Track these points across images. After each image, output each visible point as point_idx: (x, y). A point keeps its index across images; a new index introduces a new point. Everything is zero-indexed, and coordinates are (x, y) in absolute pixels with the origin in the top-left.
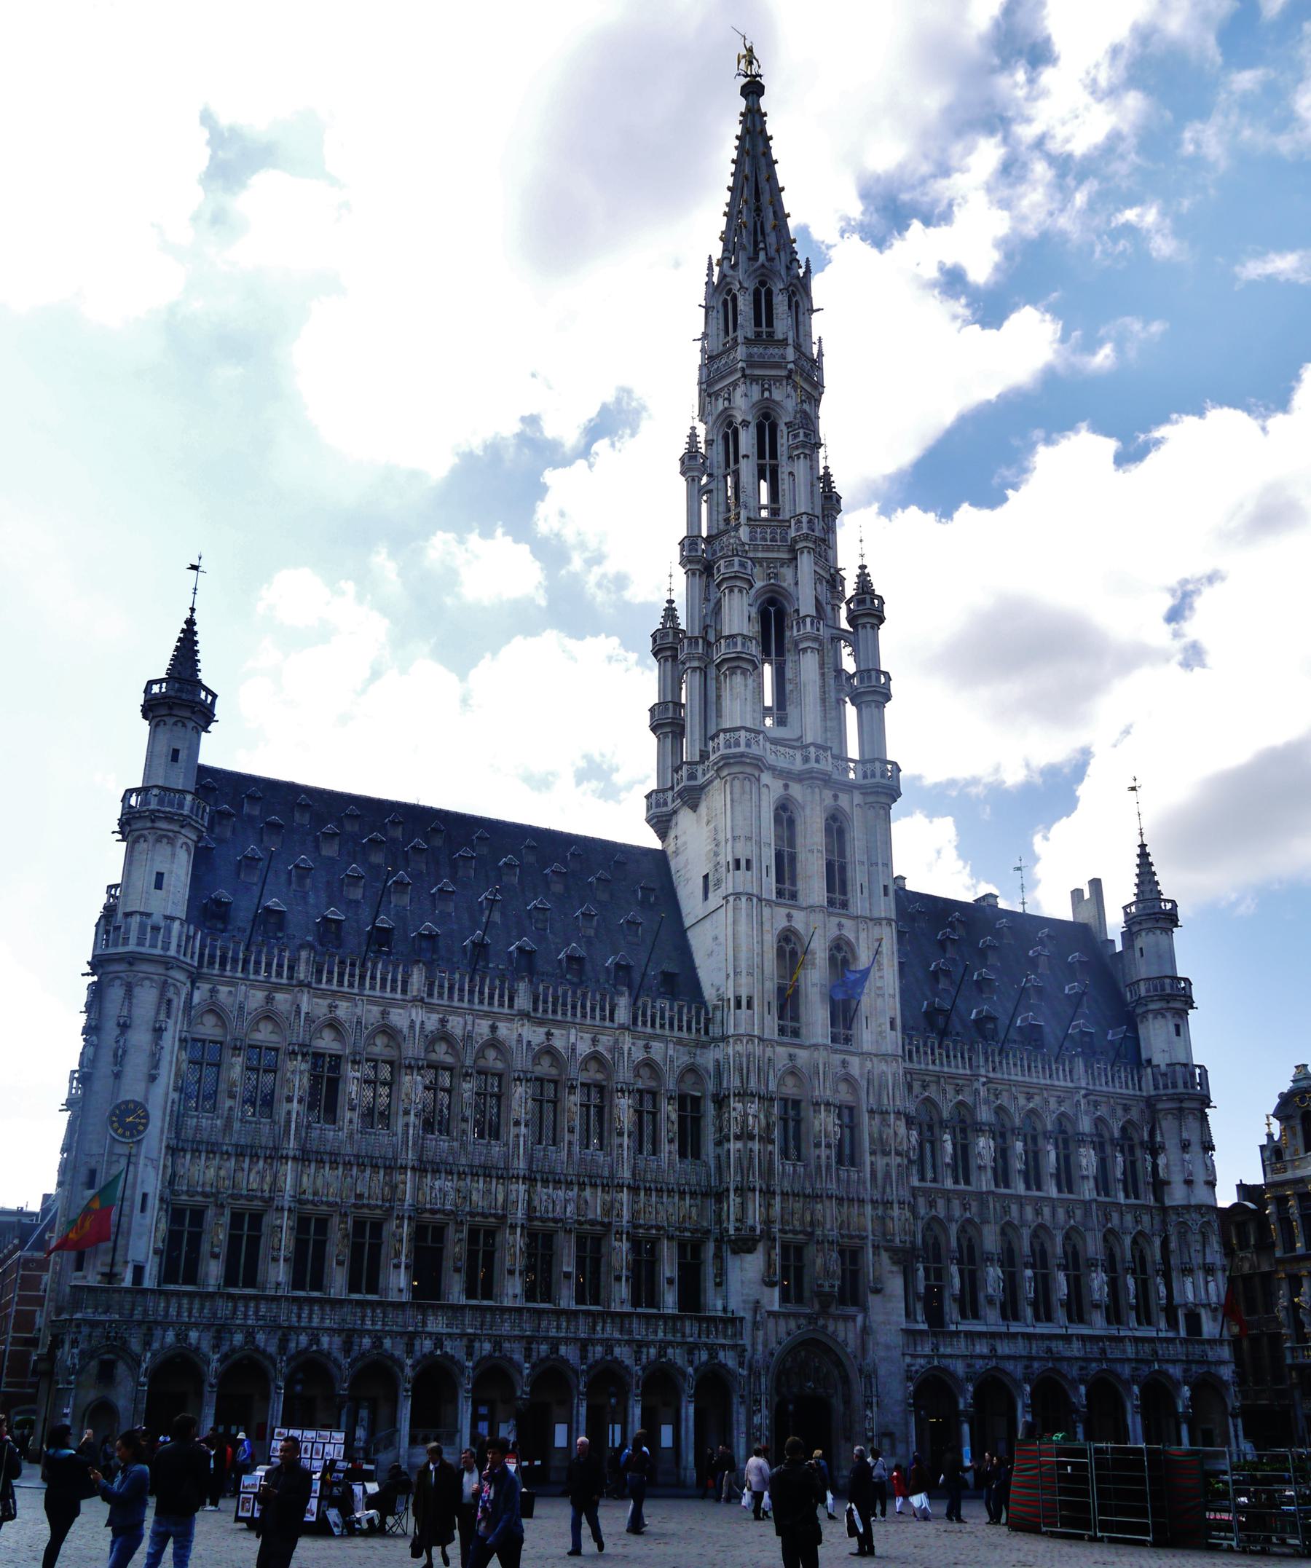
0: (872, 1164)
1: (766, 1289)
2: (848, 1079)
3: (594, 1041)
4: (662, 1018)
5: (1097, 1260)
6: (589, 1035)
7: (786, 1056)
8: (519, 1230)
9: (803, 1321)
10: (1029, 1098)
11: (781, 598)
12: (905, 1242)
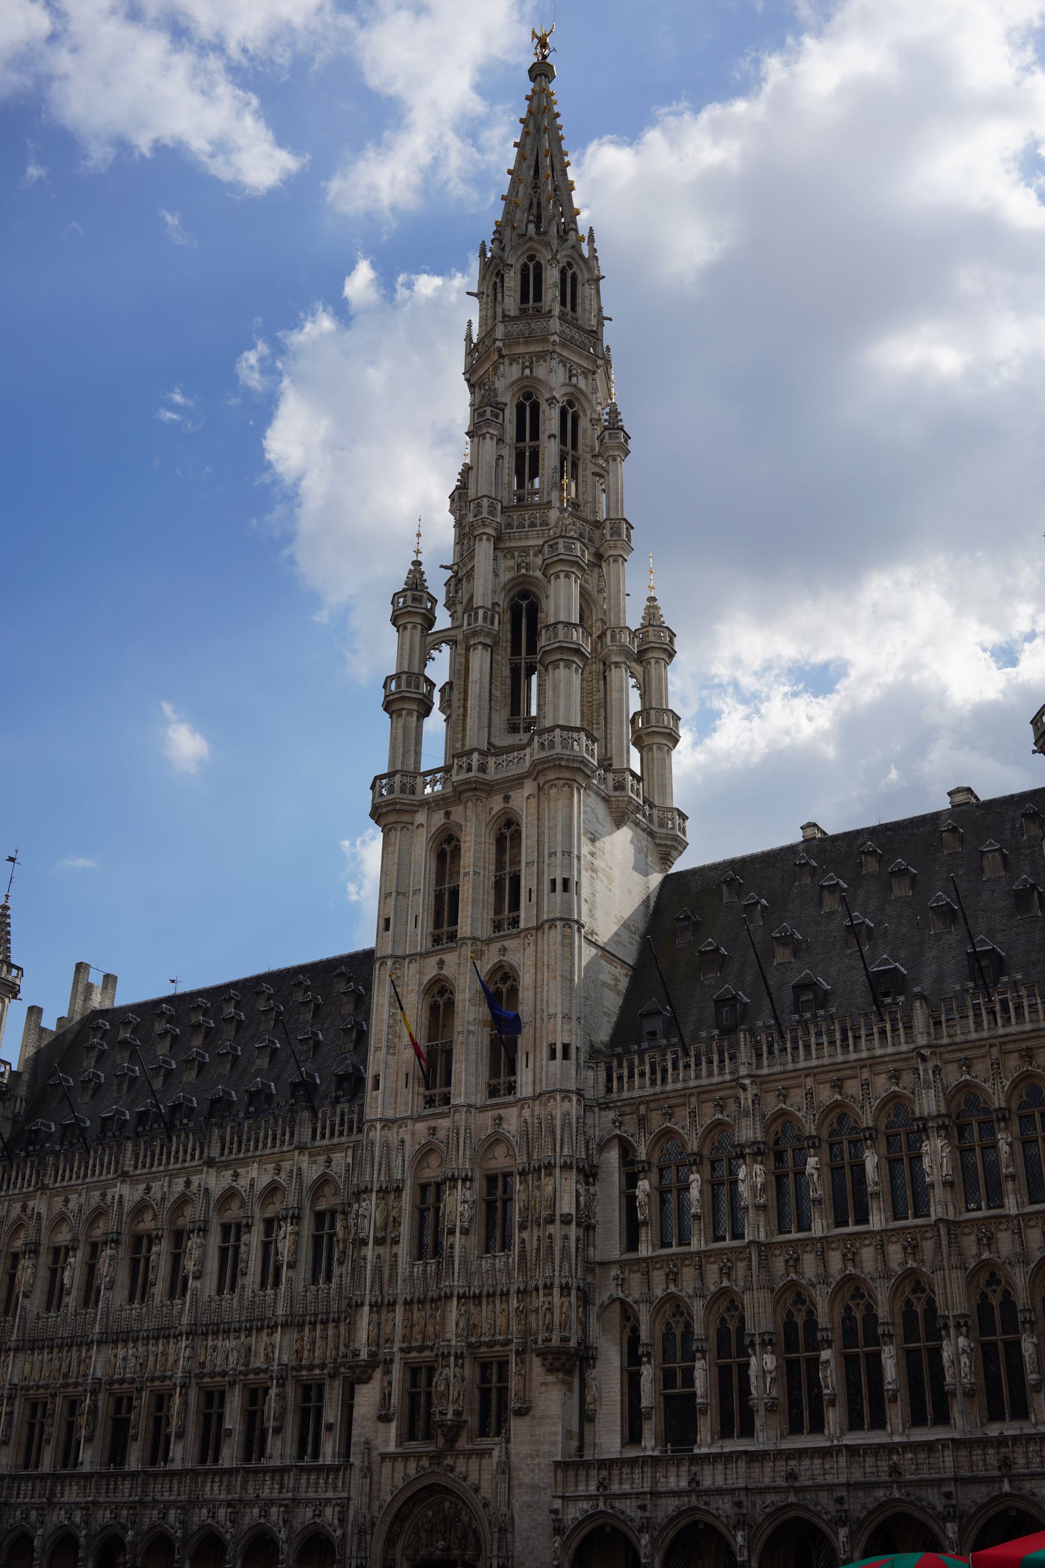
0: (523, 1242)
1: (381, 1425)
2: (497, 1139)
3: (278, 1170)
4: (342, 1124)
5: (948, 1317)
6: (273, 1165)
7: (425, 1132)
8: (178, 1389)
9: (425, 1463)
10: (838, 1085)
11: (533, 589)
12: (547, 1340)
